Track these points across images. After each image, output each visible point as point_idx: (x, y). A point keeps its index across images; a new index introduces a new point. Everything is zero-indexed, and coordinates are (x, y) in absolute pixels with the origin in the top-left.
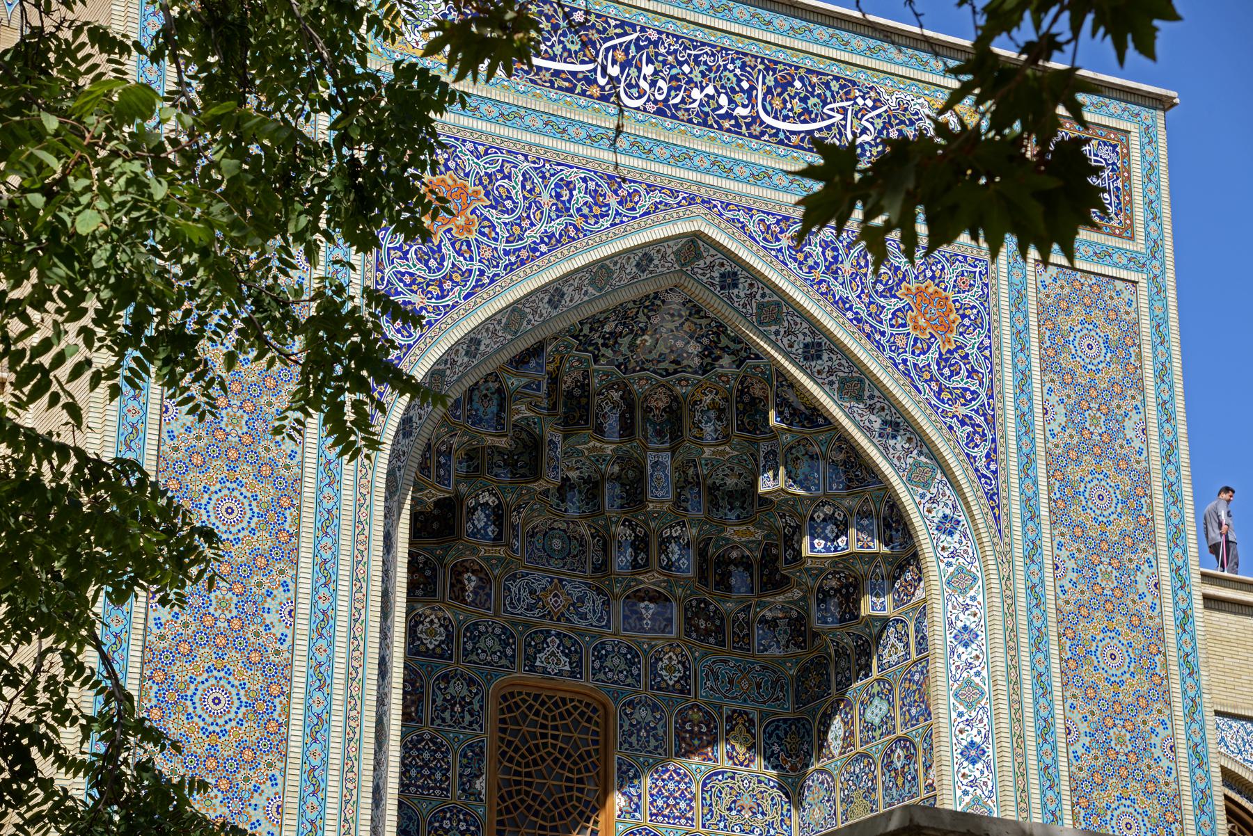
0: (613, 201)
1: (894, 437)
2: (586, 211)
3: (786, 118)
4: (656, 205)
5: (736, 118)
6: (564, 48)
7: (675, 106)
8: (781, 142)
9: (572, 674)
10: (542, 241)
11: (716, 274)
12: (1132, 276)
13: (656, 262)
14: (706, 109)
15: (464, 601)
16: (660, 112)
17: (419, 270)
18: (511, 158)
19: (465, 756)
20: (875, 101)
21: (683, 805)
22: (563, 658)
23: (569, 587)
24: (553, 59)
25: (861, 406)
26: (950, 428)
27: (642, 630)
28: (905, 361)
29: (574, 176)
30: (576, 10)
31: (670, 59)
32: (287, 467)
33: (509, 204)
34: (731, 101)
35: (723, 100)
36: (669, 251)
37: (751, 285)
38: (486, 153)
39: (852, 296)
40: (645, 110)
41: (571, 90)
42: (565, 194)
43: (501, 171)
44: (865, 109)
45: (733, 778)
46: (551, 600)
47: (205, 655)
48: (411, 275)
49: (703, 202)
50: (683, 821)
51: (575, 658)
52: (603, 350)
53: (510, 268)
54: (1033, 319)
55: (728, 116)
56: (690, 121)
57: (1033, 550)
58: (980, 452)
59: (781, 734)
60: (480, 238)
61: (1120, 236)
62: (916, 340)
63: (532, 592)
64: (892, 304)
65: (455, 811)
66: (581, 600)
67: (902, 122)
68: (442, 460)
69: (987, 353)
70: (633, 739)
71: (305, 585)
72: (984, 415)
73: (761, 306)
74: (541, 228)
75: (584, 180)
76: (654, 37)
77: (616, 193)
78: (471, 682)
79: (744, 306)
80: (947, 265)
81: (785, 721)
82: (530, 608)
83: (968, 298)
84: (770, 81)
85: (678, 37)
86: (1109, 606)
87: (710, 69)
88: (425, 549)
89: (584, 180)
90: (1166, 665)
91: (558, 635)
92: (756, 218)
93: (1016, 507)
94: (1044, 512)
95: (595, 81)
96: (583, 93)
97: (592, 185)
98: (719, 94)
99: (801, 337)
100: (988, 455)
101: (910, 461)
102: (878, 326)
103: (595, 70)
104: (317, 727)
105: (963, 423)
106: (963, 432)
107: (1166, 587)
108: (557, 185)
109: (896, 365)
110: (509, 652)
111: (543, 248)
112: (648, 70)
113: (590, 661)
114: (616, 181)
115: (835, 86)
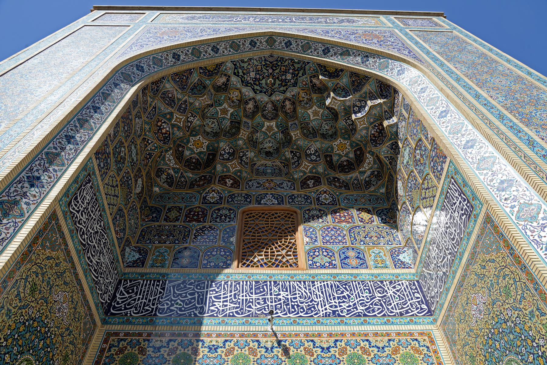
1: (368, 60)
9: (279, 204)
11: (283, 44)
13: (258, 44)
19: (226, 231)
22: (274, 200)
25: (351, 58)
27: (309, 188)
37: (296, 42)
45: (364, 228)
50: (341, 243)
52: (256, 87)
65: (219, 248)
73: (302, 47)
79: (297, 49)
88: (208, 173)
99: (320, 49)
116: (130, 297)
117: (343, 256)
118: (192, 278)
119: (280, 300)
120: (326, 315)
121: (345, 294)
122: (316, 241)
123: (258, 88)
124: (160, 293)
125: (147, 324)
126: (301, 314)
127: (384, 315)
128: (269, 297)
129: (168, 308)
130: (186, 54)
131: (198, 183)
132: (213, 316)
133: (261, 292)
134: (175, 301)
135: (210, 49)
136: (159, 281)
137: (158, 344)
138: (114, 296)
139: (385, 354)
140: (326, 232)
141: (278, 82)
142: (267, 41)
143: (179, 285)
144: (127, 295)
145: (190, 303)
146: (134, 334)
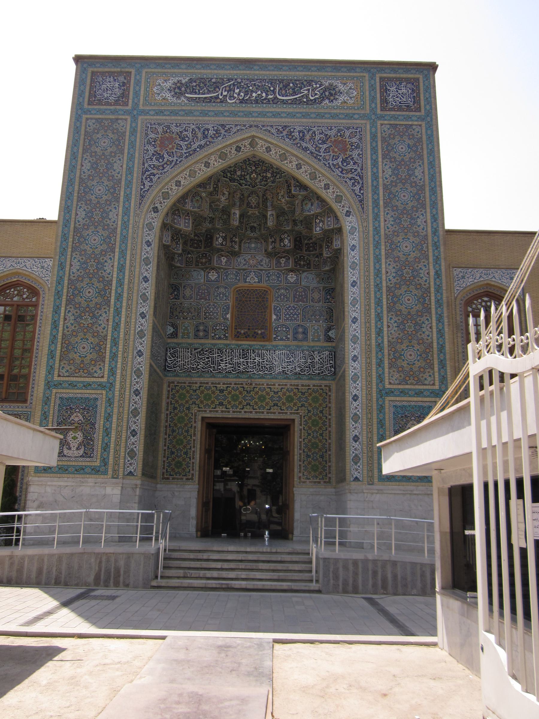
0: (223, 131)
2: (213, 136)
4: (238, 130)
5: (268, 99)
6: (208, 90)
8: (285, 103)
9: (259, 282)
10: (198, 147)
11: (264, 148)
12: (420, 123)
13: (243, 148)
15: (221, 265)
16: (241, 102)
17: (156, 163)
18: (188, 125)
19: (224, 308)
21: (295, 316)
23: (257, 257)
24: (204, 94)
26: (346, 182)
28: (329, 163)
29: (210, 127)
32: (112, 225)
33: (187, 139)
34: (266, 94)
35: (264, 95)
36: (246, 144)
38: (180, 125)
39: (309, 146)
40: (236, 103)
41: (210, 102)
42: (206, 132)
44: (316, 88)
46: (251, 262)
47: (87, 280)
49: (255, 126)
51: (260, 278)
52: (241, 181)
53: (187, 157)
54: (379, 144)
55: (265, 99)
56: (252, 103)
57: (376, 217)
58: (357, 188)
59: (330, 292)
60: (177, 150)
61: (415, 111)
62: (333, 156)
63: (245, 260)
64: (325, 146)
66: (261, 261)
67: (331, 89)
68: (187, 221)
69: (361, 156)
70: (279, 299)
71: (117, 258)
72: (359, 176)
73: (280, 155)
74: (197, 144)
75: (213, 127)
76: (239, 81)
78: (226, 288)
80: (346, 131)
81: (332, 289)
82: (244, 265)
83: (354, 140)
84: (281, 86)
85: (248, 79)
86: (406, 231)
87: (259, 86)
88: (208, 252)
89: (213, 127)
90: (427, 247)
91: (254, 272)
92: (275, 128)
93: (370, 204)
94: (381, 203)
96: (214, 102)
97: (216, 128)
98: (262, 93)
100: (360, 189)
101: (335, 195)
102: (319, 154)
103: (219, 95)
104: (119, 297)
105: (351, 180)
106: (350, 183)
107: (429, 222)
108: (204, 130)
109: (325, 165)
110: (238, 278)
111: (198, 149)
112: (237, 91)
113: (265, 278)
114: (223, 126)
115: (305, 83)
116: (175, 360)
117: (295, 331)
118: (207, 347)
119: (255, 363)
120: (279, 373)
121: (291, 360)
122: (280, 318)
123: (244, 182)
124: (191, 357)
125: (187, 376)
126: (266, 372)
127: (310, 374)
128: (250, 360)
129: (196, 367)
130: (185, 178)
131: (201, 260)
132: (220, 372)
133: (246, 357)
134: (199, 362)
135: (203, 165)
136: (188, 349)
137: (194, 388)
138: (166, 360)
139: (304, 396)
140: (288, 311)
141: (260, 177)
142: (250, 144)
143: (200, 352)
144: (173, 359)
145: (208, 364)
146: (181, 383)
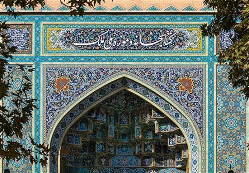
2: (95, 78)
3: (148, 43)
6: (90, 39)
7: (118, 47)
8: (146, 49)
14: (127, 45)
16: (114, 49)
20: (172, 32)
26: (190, 113)
29: (92, 70)
30: (92, 29)
31: (117, 35)
34: (133, 42)
39: (165, 85)
42: (90, 75)
43: (74, 73)
44: (169, 35)
48: (54, 102)
55: (132, 46)
56: (122, 49)
67: (180, 36)
69: (201, 92)
74: (84, 85)
75: (95, 71)
77: (103, 72)
84: (144, 34)
85: (119, 29)
86: (231, 150)
89: (95, 71)
95: (98, 45)
97: (97, 71)
100: (200, 118)
103: (98, 43)
108: (88, 73)
109: (176, 100)
111: (85, 89)
115: (161, 31)
